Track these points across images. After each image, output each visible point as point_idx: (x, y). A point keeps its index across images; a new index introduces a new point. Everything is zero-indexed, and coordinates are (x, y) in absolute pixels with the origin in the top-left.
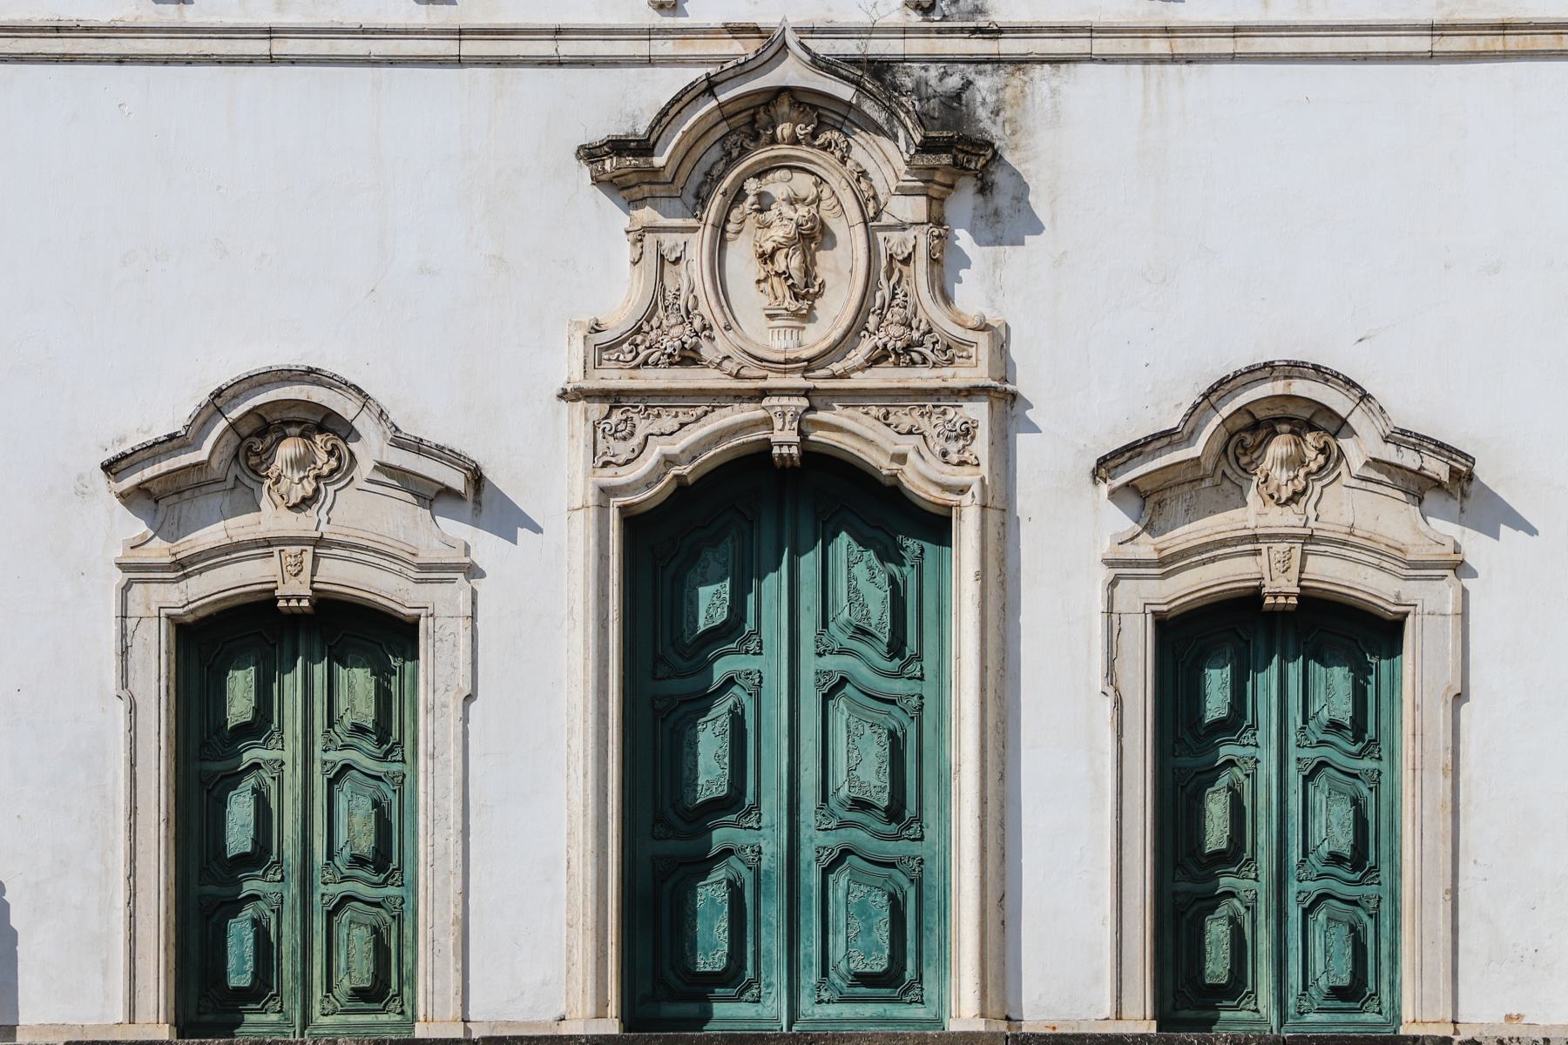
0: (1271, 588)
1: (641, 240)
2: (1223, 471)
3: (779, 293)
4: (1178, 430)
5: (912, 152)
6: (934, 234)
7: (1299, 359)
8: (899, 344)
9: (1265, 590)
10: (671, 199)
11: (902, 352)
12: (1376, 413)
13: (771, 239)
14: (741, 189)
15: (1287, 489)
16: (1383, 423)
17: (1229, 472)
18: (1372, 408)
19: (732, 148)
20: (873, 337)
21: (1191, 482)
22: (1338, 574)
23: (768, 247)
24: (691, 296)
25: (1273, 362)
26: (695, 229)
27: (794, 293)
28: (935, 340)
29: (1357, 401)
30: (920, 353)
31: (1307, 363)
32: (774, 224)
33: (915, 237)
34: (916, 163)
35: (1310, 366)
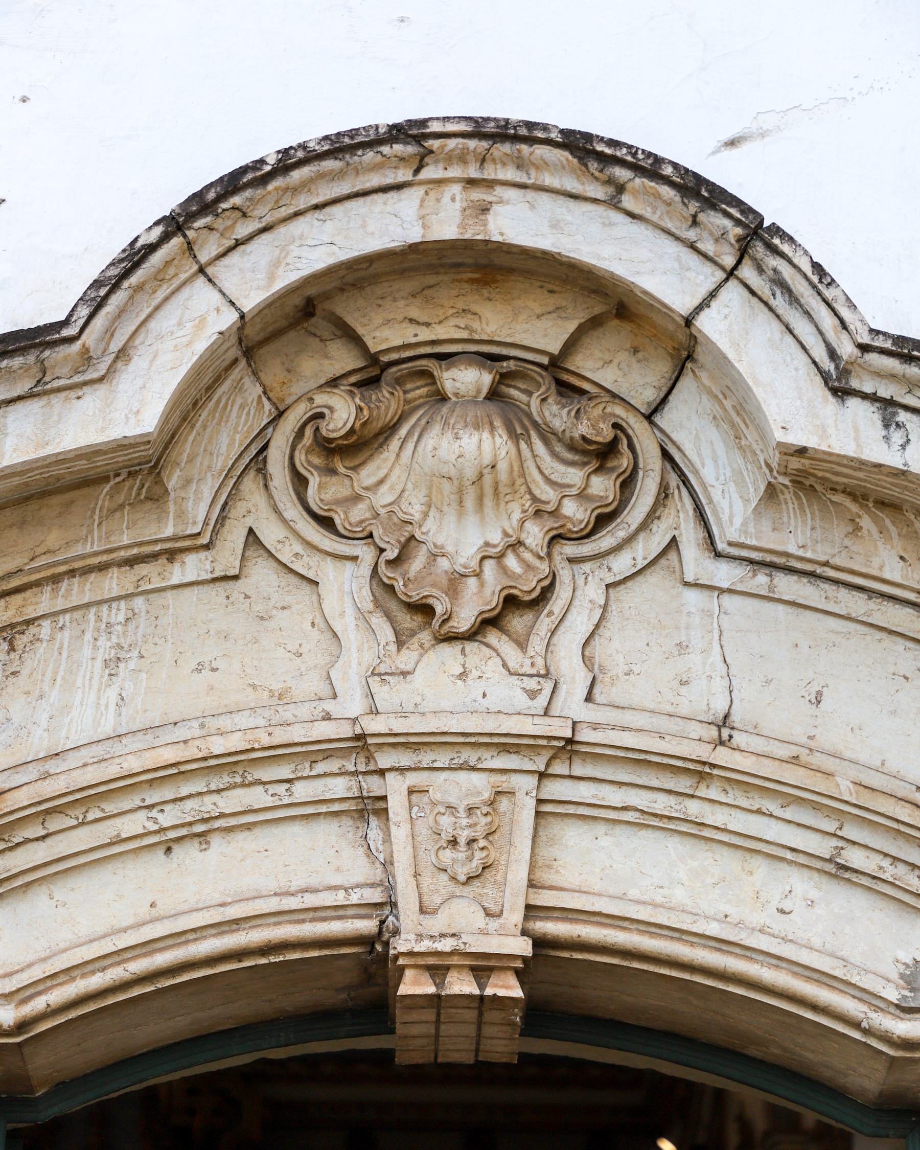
0: (420, 937)
2: (251, 531)
4: (66, 332)
7: (516, 112)
9: (401, 945)
12: (800, 287)
15: (482, 585)
16: (827, 321)
17: (270, 533)
18: (787, 272)
21: (131, 562)
22: (679, 895)
25: (424, 123)
29: (729, 261)
31: (545, 127)
35: (554, 135)
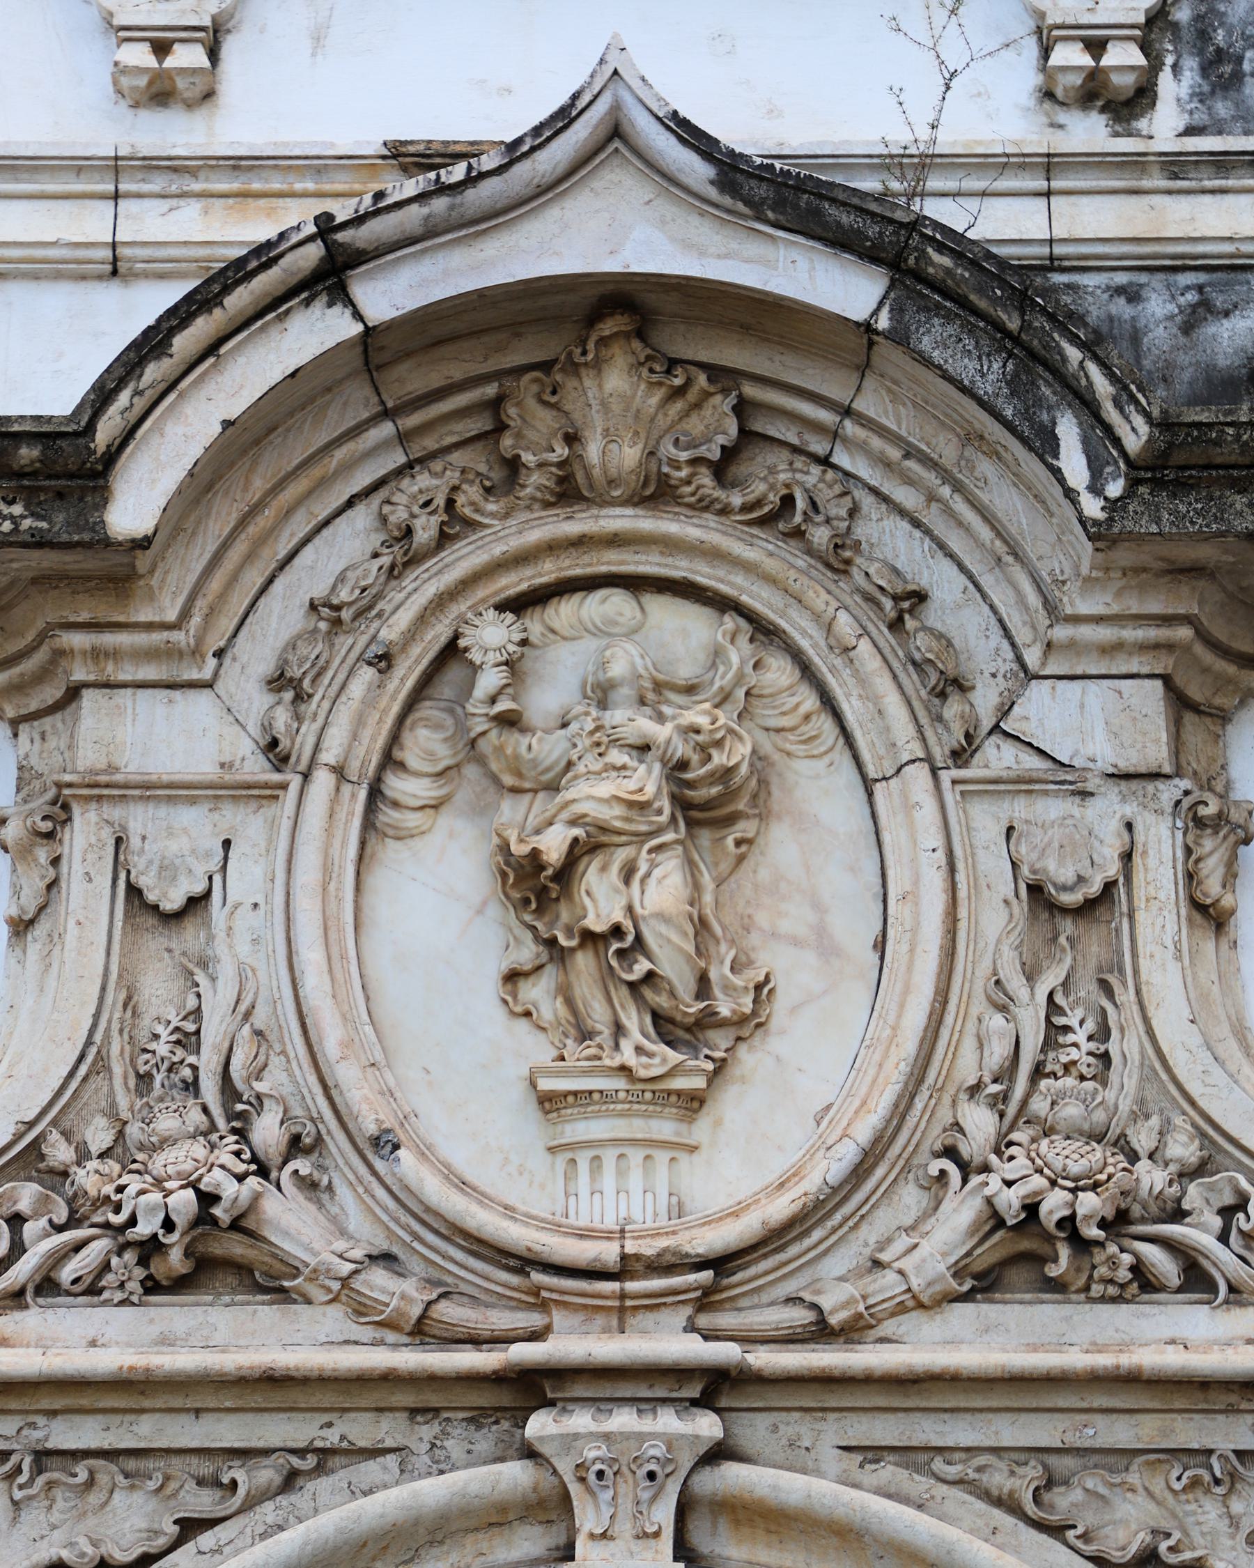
1: (50, 835)
3: (598, 1015)
5: (1115, 489)
6: (1203, 811)
8: (1088, 1203)
10: (177, 695)
11: (1094, 1232)
13: (565, 815)
14: (452, 651)
19: (413, 516)
20: (975, 1180)
23: (554, 844)
24: (247, 1028)
26: (272, 793)
27: (657, 1017)
28: (1228, 1199)
30: (1167, 1244)
32: (581, 768)
33: (1129, 826)
34: (1129, 525)
